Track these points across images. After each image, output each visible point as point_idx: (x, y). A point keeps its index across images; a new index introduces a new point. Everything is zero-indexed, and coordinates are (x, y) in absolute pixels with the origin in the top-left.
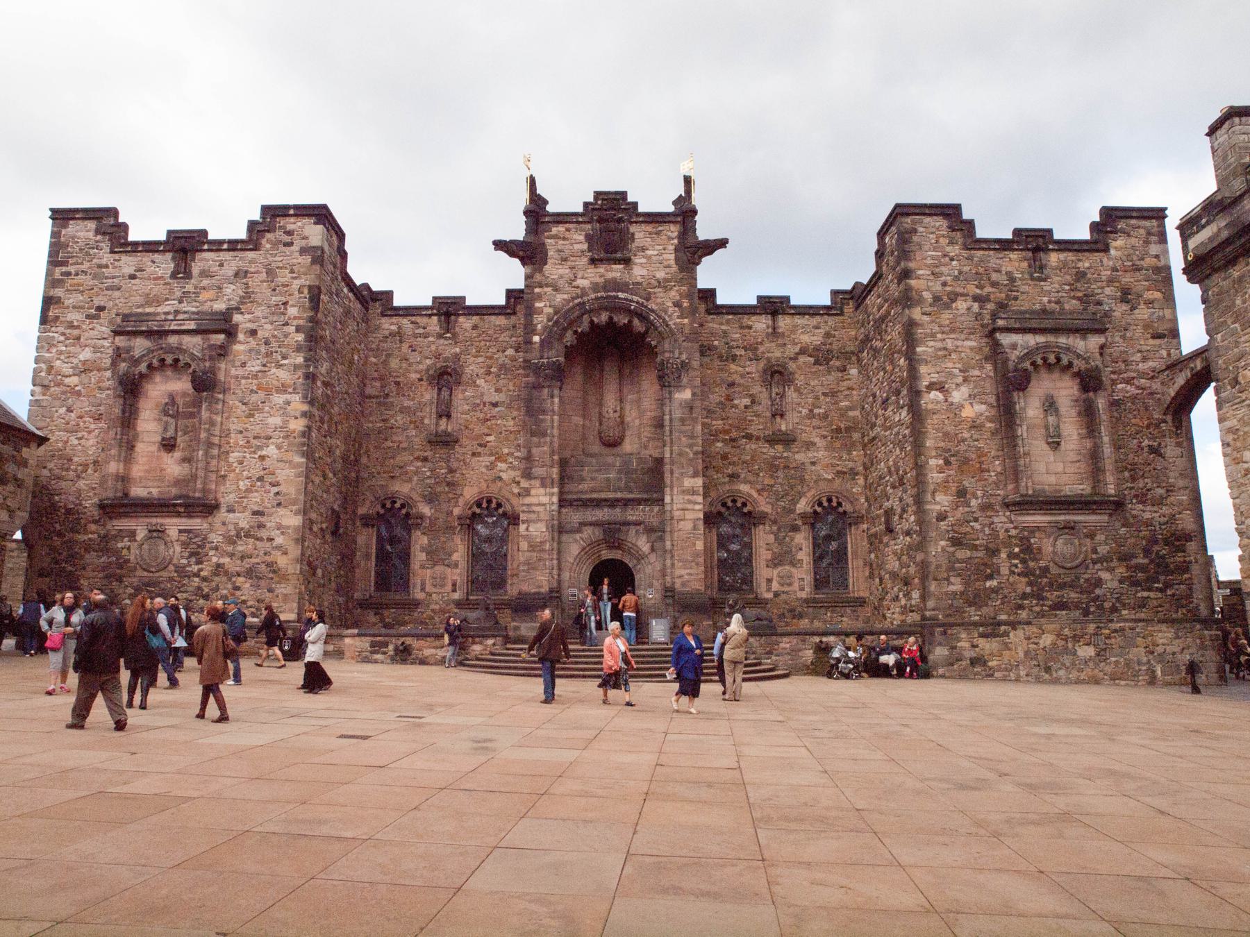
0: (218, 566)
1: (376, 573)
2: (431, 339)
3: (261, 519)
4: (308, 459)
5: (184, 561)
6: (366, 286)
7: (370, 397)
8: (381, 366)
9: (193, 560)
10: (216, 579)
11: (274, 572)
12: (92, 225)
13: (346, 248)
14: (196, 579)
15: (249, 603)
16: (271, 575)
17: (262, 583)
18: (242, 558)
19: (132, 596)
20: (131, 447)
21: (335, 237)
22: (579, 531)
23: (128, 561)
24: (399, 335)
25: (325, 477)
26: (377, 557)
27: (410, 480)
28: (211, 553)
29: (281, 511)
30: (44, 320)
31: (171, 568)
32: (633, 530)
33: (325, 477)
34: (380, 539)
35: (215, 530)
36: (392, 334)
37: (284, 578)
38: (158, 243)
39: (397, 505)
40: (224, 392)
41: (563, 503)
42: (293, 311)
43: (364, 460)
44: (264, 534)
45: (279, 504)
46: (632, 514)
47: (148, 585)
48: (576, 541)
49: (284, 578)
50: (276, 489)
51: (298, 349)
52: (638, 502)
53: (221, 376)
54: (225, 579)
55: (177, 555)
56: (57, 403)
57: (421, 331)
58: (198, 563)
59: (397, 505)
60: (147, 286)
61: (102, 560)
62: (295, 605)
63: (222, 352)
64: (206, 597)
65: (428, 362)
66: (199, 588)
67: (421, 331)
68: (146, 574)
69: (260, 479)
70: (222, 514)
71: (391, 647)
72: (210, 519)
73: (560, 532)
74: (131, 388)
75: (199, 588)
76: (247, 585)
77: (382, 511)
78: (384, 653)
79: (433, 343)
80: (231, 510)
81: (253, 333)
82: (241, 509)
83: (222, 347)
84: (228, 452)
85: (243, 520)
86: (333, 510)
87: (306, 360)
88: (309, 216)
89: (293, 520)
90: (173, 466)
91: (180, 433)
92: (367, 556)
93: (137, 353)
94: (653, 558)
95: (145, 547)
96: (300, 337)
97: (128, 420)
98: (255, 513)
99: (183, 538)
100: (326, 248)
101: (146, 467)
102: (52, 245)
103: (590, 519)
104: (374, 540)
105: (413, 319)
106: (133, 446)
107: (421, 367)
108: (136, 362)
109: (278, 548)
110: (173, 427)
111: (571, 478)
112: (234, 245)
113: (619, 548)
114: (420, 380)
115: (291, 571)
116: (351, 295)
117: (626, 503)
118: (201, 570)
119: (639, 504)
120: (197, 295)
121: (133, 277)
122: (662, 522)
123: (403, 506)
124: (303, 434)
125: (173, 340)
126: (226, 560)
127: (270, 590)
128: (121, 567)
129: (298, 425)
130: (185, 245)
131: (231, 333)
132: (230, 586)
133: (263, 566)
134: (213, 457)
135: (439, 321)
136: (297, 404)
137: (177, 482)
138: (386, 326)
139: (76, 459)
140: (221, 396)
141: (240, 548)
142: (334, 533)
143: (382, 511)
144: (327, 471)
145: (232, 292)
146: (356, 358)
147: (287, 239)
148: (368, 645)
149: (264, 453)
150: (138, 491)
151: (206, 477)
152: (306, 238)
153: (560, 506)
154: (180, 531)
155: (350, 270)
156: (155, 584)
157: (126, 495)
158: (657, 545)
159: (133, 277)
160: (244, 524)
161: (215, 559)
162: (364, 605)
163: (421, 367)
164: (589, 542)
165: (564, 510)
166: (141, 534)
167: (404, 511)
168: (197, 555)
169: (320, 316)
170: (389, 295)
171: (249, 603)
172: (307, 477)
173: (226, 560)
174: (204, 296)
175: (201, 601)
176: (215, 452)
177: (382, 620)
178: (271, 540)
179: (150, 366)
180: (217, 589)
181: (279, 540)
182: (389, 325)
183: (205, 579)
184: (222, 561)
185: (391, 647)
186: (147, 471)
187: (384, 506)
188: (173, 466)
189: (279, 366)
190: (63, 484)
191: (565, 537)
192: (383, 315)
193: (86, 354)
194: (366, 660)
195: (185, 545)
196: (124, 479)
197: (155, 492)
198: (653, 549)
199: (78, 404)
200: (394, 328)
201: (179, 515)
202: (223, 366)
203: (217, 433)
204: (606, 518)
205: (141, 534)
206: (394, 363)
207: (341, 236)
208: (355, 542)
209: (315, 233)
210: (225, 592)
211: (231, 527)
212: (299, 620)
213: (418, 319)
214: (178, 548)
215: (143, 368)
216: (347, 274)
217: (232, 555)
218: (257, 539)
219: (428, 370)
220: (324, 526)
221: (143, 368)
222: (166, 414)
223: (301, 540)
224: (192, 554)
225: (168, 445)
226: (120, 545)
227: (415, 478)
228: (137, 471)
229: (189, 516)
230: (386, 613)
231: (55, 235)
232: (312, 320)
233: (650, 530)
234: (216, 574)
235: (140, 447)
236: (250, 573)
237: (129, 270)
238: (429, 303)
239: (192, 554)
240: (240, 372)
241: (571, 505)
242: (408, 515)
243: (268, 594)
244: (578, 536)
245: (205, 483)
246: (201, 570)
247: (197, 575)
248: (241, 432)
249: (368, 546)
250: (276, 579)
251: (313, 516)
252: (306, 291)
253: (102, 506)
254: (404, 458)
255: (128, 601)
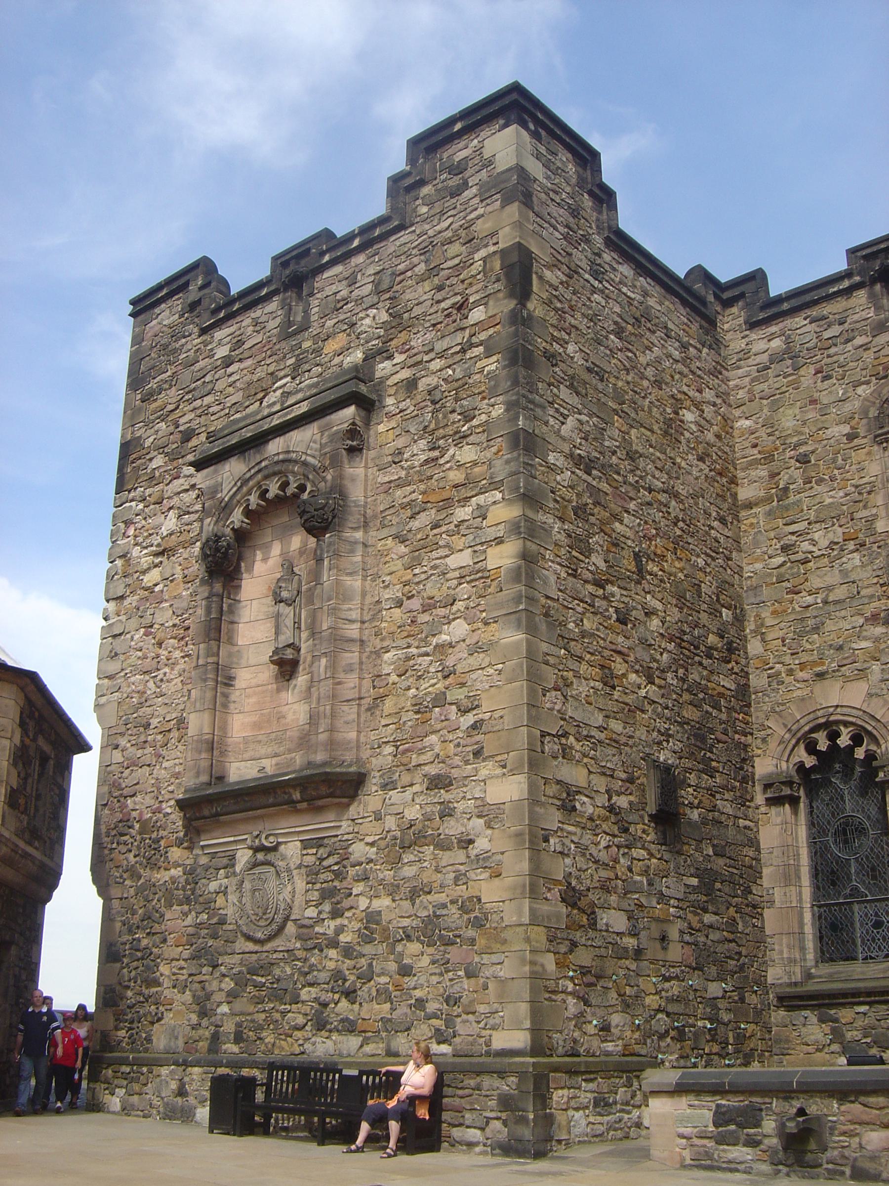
0: (372, 917)
1: (819, 918)
2: (859, 341)
3: (444, 795)
4: (531, 629)
5: (311, 912)
6: (701, 273)
7: (749, 505)
8: (762, 433)
9: (327, 907)
10: (368, 949)
11: (478, 924)
12: (177, 303)
13: (607, 178)
14: (333, 953)
15: (432, 1007)
16: (471, 933)
17: (455, 954)
18: (414, 894)
19: (232, 996)
20: (229, 682)
21: (564, 157)
23: (222, 922)
24: (790, 354)
25: (609, 680)
26: (816, 873)
27: (862, 674)
28: (358, 888)
29: (486, 769)
30: (121, 487)
31: (291, 928)
33: (609, 680)
34: (816, 828)
35: (361, 829)
36: (776, 358)
37: (498, 937)
38: (260, 285)
39: (844, 741)
40: (366, 525)
42: (477, 315)
43: (754, 647)
44: (452, 828)
45: (477, 754)
47: (253, 972)
49: (498, 937)
50: (469, 720)
51: (494, 392)
53: (357, 494)
54: (382, 948)
55: (299, 900)
56: (134, 623)
57: (835, 330)
58: (336, 913)
59: (844, 741)
60: (242, 372)
61: (189, 920)
62: (524, 1008)
63: (354, 443)
64: (350, 994)
65: (860, 390)
66: (338, 975)
67: (835, 330)
68: (251, 946)
69: (440, 700)
70: (371, 799)
71: (769, 1125)
72: (353, 810)
74: (223, 564)
75: (338, 975)
76: (425, 961)
77: (810, 761)
78: (752, 1143)
79: (865, 347)
80: (387, 786)
81: (411, 385)
82: (406, 779)
83: (353, 432)
84: (378, 654)
85: (410, 804)
86: (656, 765)
87: (510, 406)
88: (488, 120)
89: (508, 790)
90: (294, 707)
91: (304, 635)
92: (789, 877)
93: (225, 494)
95: (247, 885)
96: (492, 364)
97: (217, 627)
98: (438, 783)
99: (310, 860)
100: (536, 169)
101: (254, 718)
102: (133, 355)
104: (802, 832)
105: (814, 312)
106: (232, 678)
107: (847, 407)
108: (225, 509)
109: (482, 861)
110: (289, 622)
112: (371, 236)
114: (851, 437)
115: (510, 918)
116: (656, 290)
118: (340, 930)
120: (318, 352)
121: (228, 362)
123: (857, 740)
124: (516, 575)
125: (275, 447)
126: (383, 903)
127: (470, 974)
128: (215, 936)
129: (502, 557)
130: (296, 271)
131: (368, 406)
132: (393, 966)
133: (453, 909)
134: (349, 669)
135: (872, 297)
136: (503, 512)
137: (304, 741)
138: (762, 345)
139: (154, 722)
140: (359, 535)
141: (408, 871)
142: (667, 819)
143: (810, 761)
144: (619, 667)
145: (373, 320)
146: (689, 416)
147: (455, 181)
148: (709, 1115)
149: (444, 637)
150: (241, 770)
151: (333, 715)
152: (490, 162)
154: (306, 844)
155: (629, 220)
156: (265, 968)
157: (221, 779)
159: (228, 362)
160: (413, 813)
161: (363, 903)
162: (793, 1001)
163: (847, 407)
166: (244, 857)
167: (860, 753)
168: (334, 898)
169: (534, 306)
170: (757, 278)
171: (432, 1007)
172: (533, 678)
173: (383, 903)
174: (332, 346)
175: (344, 1004)
176: (352, 657)
177: (837, 1035)
178: (467, 842)
179: (248, 513)
180: (367, 976)
181: (482, 844)
182: (765, 343)
183: (348, 952)
184: (377, 904)
185: (769, 1125)
186: (257, 726)
187: (811, 748)
188: (294, 707)
189: (461, 439)
190: (141, 773)
192: (753, 325)
193: (170, 523)
194: (704, 1163)
195: (312, 874)
196: (214, 746)
197: (270, 766)
199: (159, 619)
200: (777, 343)
201: (291, 807)
202: (360, 471)
203: (354, 615)
205: (244, 857)
206: (788, 420)
207: (587, 158)
208: (754, 843)
209: (504, 145)
210: (384, 980)
211: (391, 823)
212: (537, 1049)
213: (827, 309)
214: (300, 884)
215: (237, 517)
216: (620, 234)
217: (393, 890)
218: (443, 845)
219: (865, 412)
220: (622, 802)
221: (237, 517)
222: (279, 600)
223: (536, 839)
224: (327, 894)
225: (286, 666)
226: (213, 886)
227: (876, 667)
228: (239, 726)
229: (315, 809)
230: (845, 1015)
231: (137, 340)
232: (520, 320)
234: (369, 940)
235: (244, 678)
236: (431, 931)
237: (222, 352)
238: (841, 265)
239: (327, 894)
240: (395, 473)
242: (871, 756)
243: (466, 983)
245: (332, 730)
246: (340, 930)
247: (334, 943)
248: (399, 604)
249: (789, 849)
250: (481, 942)
251: (575, 775)
252: (497, 264)
253: (182, 805)
254: (840, 625)
255: (225, 1009)
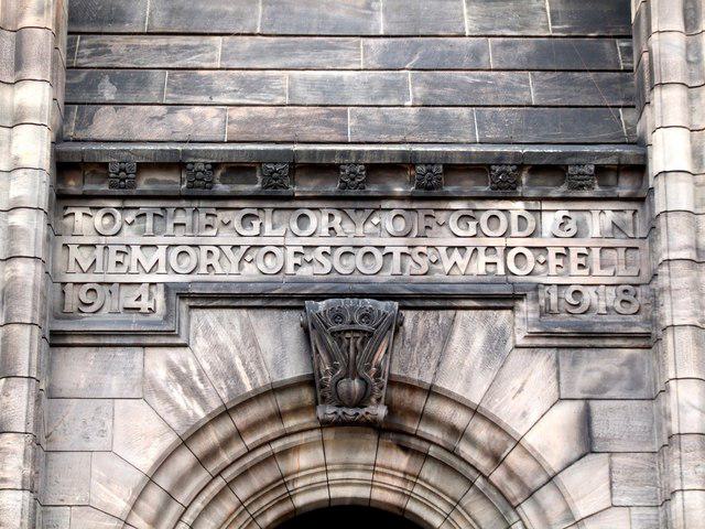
22: (165, 337)
32: (471, 331)
41: (79, 175)
46: (462, 246)
48: (147, 390)
52: (497, 177)
73: (57, 340)
94: (587, 487)
103: (229, 272)
111: (132, 78)
113: (391, 431)
117: (433, 181)
119: (506, 190)
122: (644, 291)
153: (62, 200)
158: (612, 420)
164: (218, 396)
165: (84, 222)
191: (79, 368)
198: (587, 442)
204: (316, 270)
233: (572, 336)
241: (126, 195)
244: (157, 363)
